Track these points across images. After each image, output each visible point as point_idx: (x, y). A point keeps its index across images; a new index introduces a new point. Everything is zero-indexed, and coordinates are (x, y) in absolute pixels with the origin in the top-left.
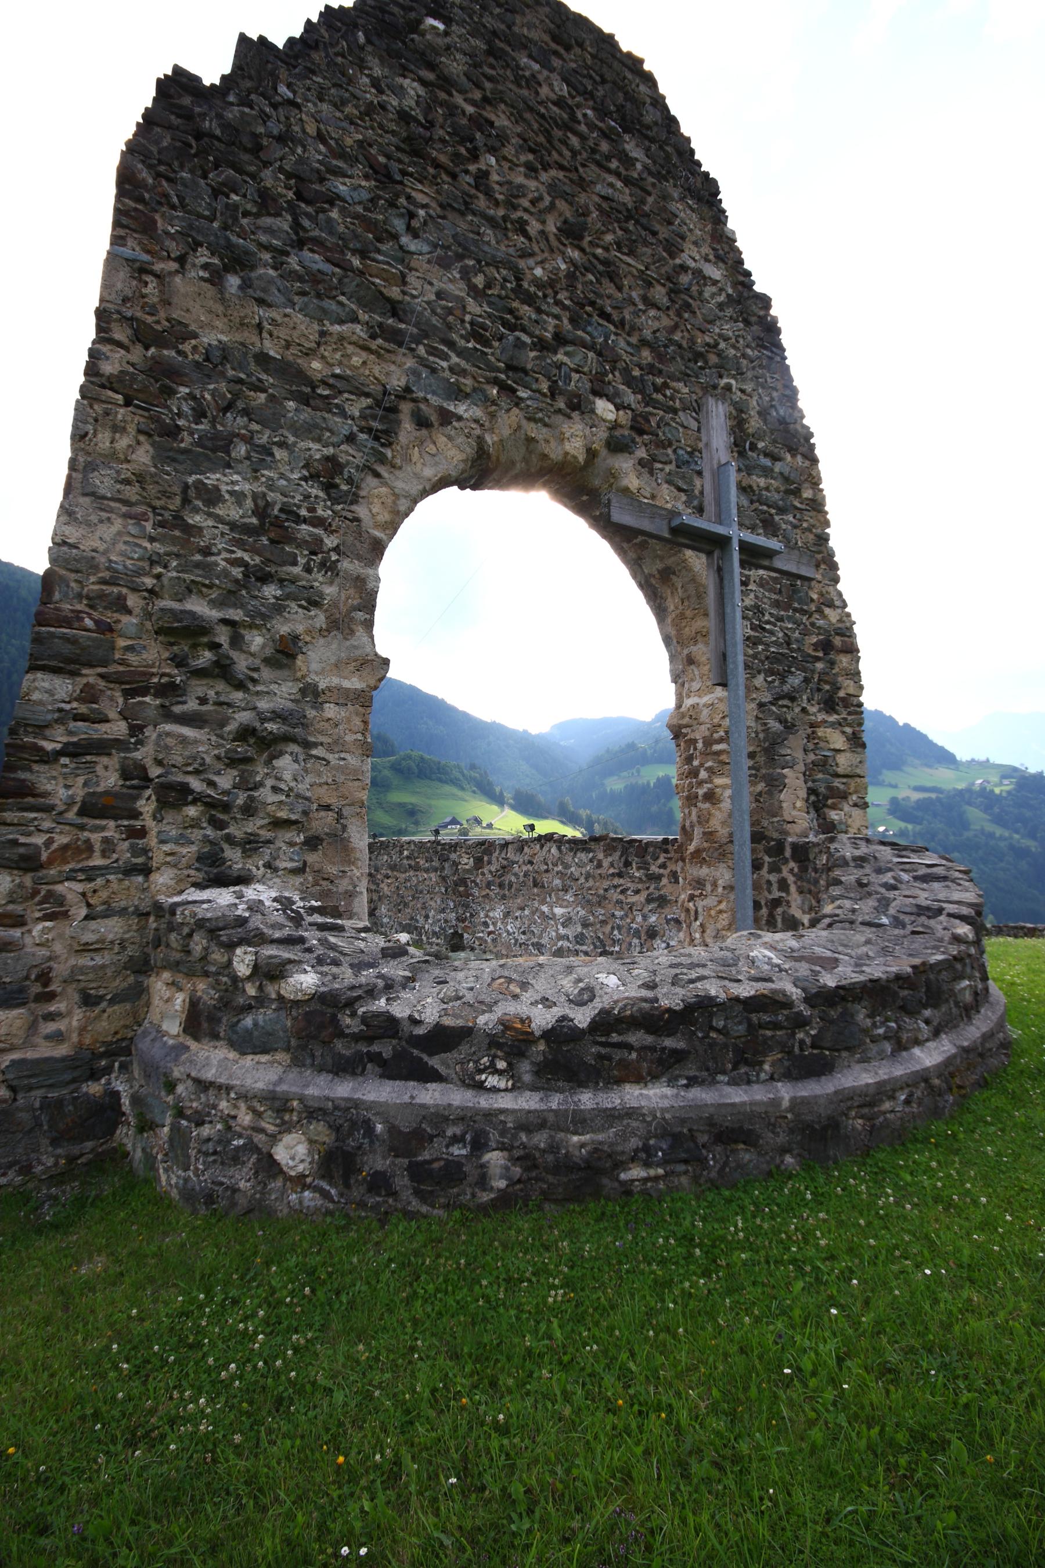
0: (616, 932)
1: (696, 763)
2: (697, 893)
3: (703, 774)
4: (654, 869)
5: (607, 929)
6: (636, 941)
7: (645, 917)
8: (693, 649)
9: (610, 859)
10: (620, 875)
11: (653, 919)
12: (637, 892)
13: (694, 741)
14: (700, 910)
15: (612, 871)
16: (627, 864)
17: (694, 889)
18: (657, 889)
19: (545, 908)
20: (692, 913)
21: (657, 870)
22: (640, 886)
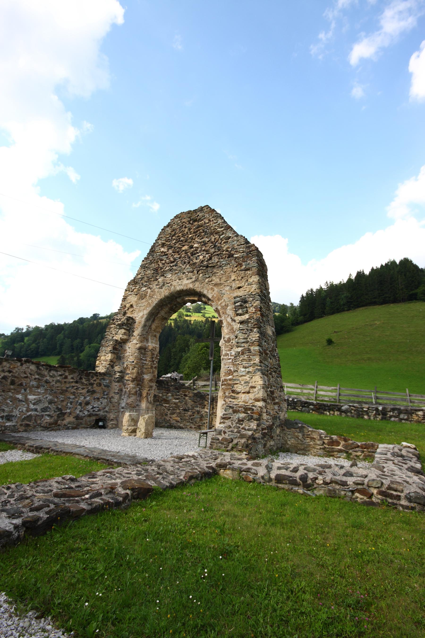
0: (69, 404)
1: (154, 359)
3: (155, 362)
5: (64, 403)
6: (79, 407)
7: (85, 398)
8: (157, 334)
9: (71, 376)
10: (77, 382)
11: (88, 398)
12: (83, 389)
13: (154, 354)
15: (72, 380)
16: (81, 378)
18: (92, 388)
19: (20, 396)
21: (93, 382)
22: (85, 387)
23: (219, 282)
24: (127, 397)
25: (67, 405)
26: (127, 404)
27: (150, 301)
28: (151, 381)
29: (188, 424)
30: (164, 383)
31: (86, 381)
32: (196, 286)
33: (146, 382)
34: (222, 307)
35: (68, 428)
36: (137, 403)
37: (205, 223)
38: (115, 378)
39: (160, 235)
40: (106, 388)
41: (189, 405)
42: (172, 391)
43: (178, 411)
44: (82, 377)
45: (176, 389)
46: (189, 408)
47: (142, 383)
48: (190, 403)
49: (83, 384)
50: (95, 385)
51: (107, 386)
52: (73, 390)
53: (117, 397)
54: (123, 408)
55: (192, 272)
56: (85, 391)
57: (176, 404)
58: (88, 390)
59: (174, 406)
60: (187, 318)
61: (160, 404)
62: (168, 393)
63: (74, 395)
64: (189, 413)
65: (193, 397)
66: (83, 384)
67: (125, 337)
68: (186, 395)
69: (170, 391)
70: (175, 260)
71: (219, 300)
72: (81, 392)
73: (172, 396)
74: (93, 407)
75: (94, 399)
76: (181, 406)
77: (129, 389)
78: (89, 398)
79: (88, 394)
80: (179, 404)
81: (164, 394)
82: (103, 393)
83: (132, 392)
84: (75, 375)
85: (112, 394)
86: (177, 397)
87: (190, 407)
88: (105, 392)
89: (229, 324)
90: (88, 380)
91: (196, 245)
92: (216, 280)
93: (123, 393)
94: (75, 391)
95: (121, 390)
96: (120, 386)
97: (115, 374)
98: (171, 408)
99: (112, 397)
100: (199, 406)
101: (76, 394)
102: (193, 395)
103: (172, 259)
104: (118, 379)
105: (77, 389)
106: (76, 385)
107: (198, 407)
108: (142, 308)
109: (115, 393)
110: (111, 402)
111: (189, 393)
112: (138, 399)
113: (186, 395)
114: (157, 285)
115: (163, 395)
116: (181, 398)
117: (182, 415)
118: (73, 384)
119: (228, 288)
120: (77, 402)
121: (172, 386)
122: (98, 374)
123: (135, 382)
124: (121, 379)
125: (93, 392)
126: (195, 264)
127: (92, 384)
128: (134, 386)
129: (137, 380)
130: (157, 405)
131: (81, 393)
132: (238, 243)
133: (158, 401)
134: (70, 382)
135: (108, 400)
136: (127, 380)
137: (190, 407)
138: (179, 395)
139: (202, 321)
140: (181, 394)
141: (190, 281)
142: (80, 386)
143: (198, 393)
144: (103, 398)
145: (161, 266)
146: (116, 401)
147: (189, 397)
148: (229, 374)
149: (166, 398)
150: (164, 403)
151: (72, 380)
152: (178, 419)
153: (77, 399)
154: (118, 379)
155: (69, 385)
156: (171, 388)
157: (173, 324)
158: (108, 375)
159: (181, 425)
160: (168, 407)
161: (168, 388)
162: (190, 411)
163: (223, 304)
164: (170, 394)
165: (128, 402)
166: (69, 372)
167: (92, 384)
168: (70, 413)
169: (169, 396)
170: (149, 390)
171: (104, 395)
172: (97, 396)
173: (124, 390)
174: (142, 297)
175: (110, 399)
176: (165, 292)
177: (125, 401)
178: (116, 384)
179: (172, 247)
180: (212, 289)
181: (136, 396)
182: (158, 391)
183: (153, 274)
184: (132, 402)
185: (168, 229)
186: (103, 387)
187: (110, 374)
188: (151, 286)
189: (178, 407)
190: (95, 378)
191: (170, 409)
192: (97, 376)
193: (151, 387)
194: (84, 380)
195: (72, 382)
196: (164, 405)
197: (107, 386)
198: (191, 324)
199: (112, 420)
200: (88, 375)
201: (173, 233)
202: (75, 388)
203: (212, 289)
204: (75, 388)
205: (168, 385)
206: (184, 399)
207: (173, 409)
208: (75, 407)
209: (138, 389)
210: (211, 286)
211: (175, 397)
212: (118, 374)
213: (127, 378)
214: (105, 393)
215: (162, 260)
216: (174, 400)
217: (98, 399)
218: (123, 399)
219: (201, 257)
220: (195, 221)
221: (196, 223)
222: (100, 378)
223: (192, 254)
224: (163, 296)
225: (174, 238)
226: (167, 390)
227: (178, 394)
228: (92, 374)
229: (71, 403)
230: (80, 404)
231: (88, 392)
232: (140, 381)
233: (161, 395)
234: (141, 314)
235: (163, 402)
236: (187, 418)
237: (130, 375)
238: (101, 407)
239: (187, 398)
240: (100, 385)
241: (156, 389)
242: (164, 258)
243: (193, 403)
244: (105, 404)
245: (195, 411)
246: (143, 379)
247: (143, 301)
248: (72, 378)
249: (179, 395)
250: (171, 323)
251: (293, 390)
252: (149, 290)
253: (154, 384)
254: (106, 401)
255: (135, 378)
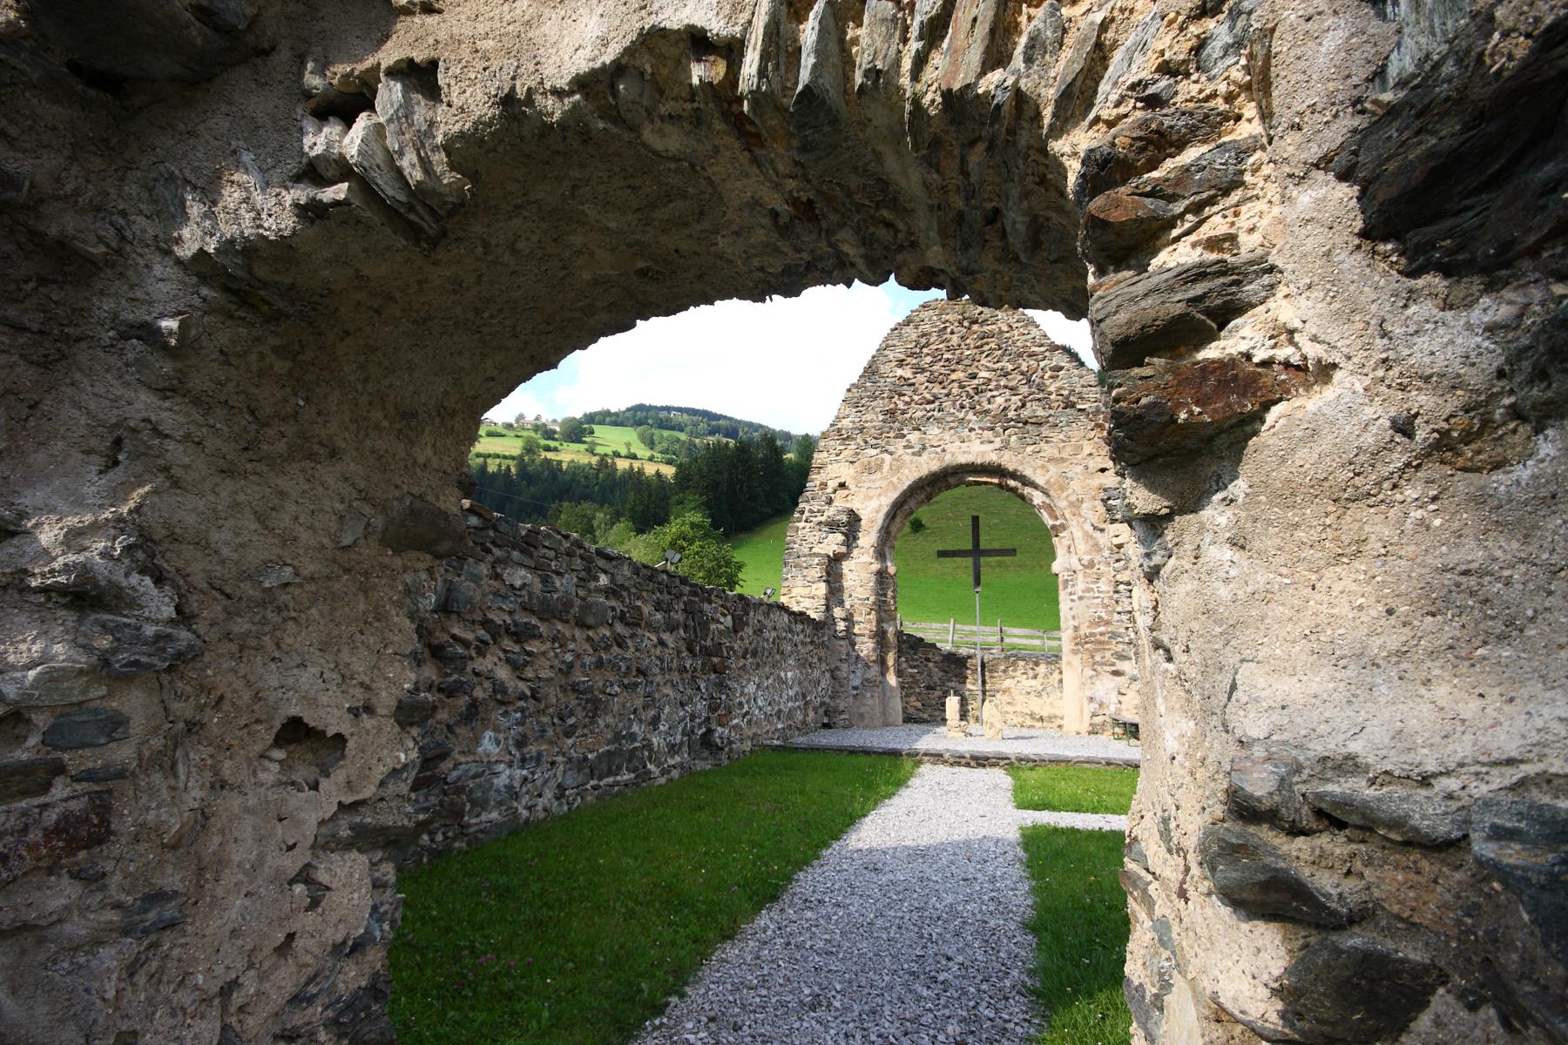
23: (1057, 455)
27: (895, 480)
32: (1006, 457)
34: (1071, 504)
37: (1001, 332)
39: (887, 339)
45: (911, 647)
48: (937, 674)
54: (855, 688)
55: (992, 429)
60: (550, 455)
64: (938, 693)
67: (844, 549)
68: (928, 660)
70: (936, 398)
71: (1062, 489)
89: (1088, 536)
91: (983, 374)
92: (1048, 450)
99: (837, 668)
103: (929, 397)
108: (873, 492)
113: (928, 660)
114: (905, 447)
119: (1079, 469)
126: (987, 412)
132: (1082, 382)
139: (590, 464)
141: (991, 447)
145: (901, 406)
148: (1098, 625)
152: (919, 704)
157: (513, 470)
159: (925, 716)
163: (1073, 498)
174: (870, 469)
176: (928, 464)
177: (859, 674)
179: (924, 370)
180: (1043, 467)
183: (884, 421)
185: (907, 329)
188: (891, 449)
189: (916, 682)
198: (560, 470)
201: (923, 341)
203: (1043, 467)
210: (1040, 462)
215: (901, 395)
219: (1000, 400)
220: (976, 322)
221: (975, 327)
223: (977, 391)
224: (924, 472)
225: (925, 350)
234: (874, 504)
242: (908, 391)
247: (872, 477)
250: (508, 468)
251: (1024, 641)
252: (887, 457)
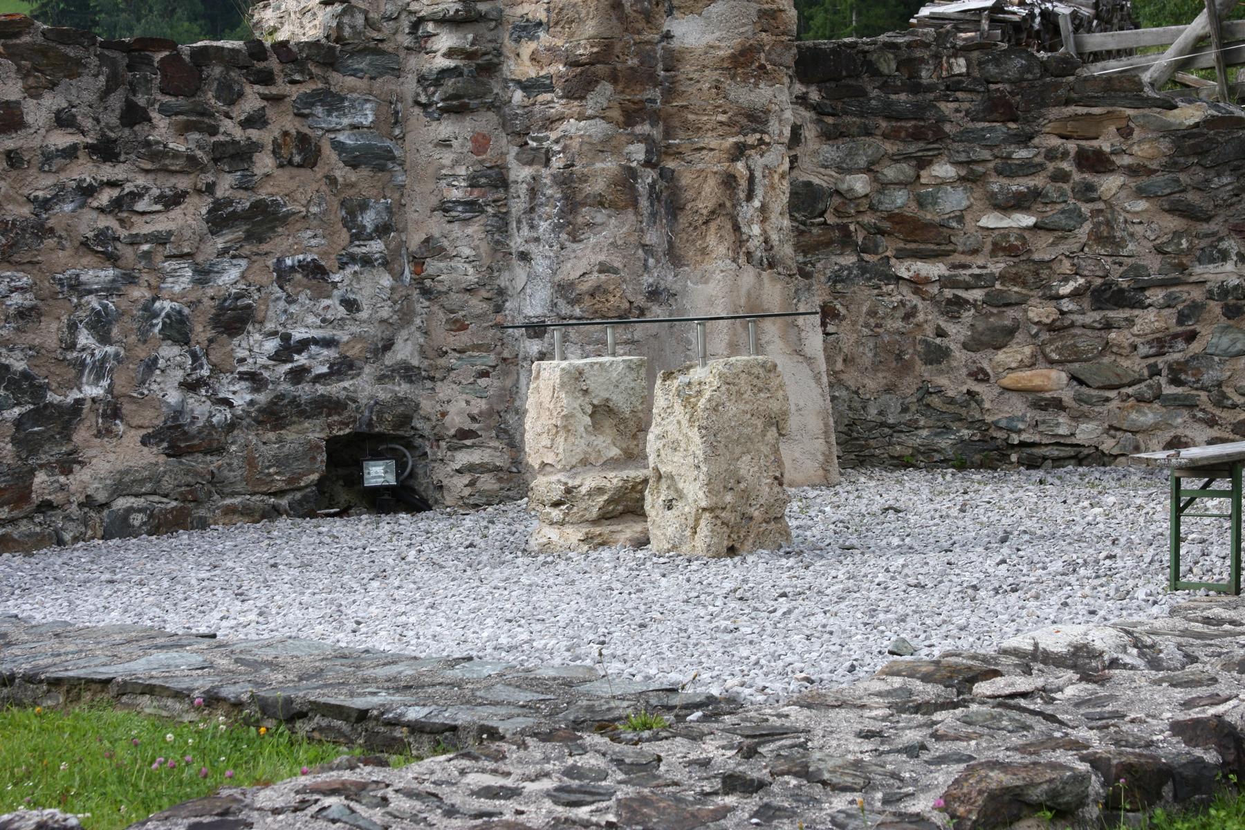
0: (84, 338)
2: (752, 139)
4: (231, 129)
5: (49, 333)
6: (169, 352)
7: (203, 275)
10: (105, 151)
11: (230, 276)
12: (172, 201)
14: (758, 174)
15: (62, 140)
16: (134, 115)
17: (743, 131)
20: (743, 184)
21: (238, 134)
22: (183, 183)
24: (557, 228)
25: (72, 346)
26: (563, 289)
28: (743, 62)
29: (1148, 416)
30: (875, 73)
31: (183, 130)
33: (699, 85)
35: (120, 528)
36: (647, 279)
38: (421, 79)
40: (365, 172)
41: (1139, 250)
42: (966, 136)
43: (1039, 311)
44: (141, 100)
45: (999, 109)
46: (1137, 270)
47: (670, 92)
48: (1145, 226)
49: (157, 157)
50: (264, 162)
51: (374, 159)
52: (90, 222)
53: (467, 240)
56: (187, 219)
57: (1011, 251)
58: (217, 205)
59: (997, 267)
61: (863, 268)
62: (923, 163)
63: (112, 259)
64: (1150, 320)
65: (1172, 165)
66: (157, 157)
68: (1096, 162)
69: (941, 136)
72: (161, 224)
73: (970, 179)
74: (288, 349)
75: (283, 275)
76: (1066, 266)
77: (557, 162)
78: (233, 274)
79: (220, 243)
80: (1043, 248)
81: (890, 172)
82: (350, 221)
83: (598, 186)
84: (83, 91)
85: (422, 225)
86: (1019, 185)
87: (1153, 264)
88: (364, 206)
90: (201, 121)
93: (518, 206)
94: (105, 222)
95: (500, 181)
96: (480, 143)
97: (421, 44)
98: (977, 295)
99: (432, 248)
100: (1232, 245)
101: (127, 252)
102: (1165, 146)
104: (450, 84)
105: (117, 205)
106: (108, 172)
107: (1224, 256)
109: (444, 207)
110: (426, 292)
111: (1125, 133)
112: (651, 238)
113: (1096, 162)
115: (883, 186)
116: (1051, 189)
117: (1086, 341)
118: (85, 171)
120: (149, 312)
121: (953, 86)
122: (274, 63)
123: (606, 88)
124: (471, 85)
125: (263, 220)
127: (239, 156)
128: (597, 128)
129: (614, 78)
130: (836, 279)
131: (161, 239)
133: (846, 240)
134: (48, 158)
135: (398, 277)
136: (530, 87)
137: (1153, 264)
138: (1028, 168)
140: (1051, 155)
142: (141, 180)
143: (1209, 122)
144: (353, 259)
146: (472, 276)
147: (1132, 171)
149: (912, 210)
150: (901, 255)
151: (62, 140)
152: (1054, 379)
153: (139, 293)
154: (450, 84)
155: (50, 180)
156: (947, 107)
158: (363, 64)
159: (1087, 433)
160: (944, 282)
161: (918, 112)
162: (1156, 295)
164: (943, 170)
165: (571, 271)
166: (25, 74)
167: (239, 156)
168: (113, 412)
169: (941, 183)
170: (739, 151)
171: (359, 235)
172: (298, 245)
173: (521, 173)
175: (418, 262)
177: (541, 265)
178: (445, 128)
181: (630, 216)
182: (829, 151)
184: (604, 268)
186: (342, 173)
187: (374, 50)
189: (1036, 277)
190: (251, 101)
191: (959, 303)
192: (266, 78)
193: (755, 119)
194: (161, 129)
195: (70, 153)
196: (903, 269)
197: (374, 159)
199: (463, 434)
200: (185, 77)
202: (105, 197)
204: (105, 197)
205: (915, 87)
206: (1087, 194)
207: (990, 300)
208: (142, 352)
209: (638, 152)
211: (996, 184)
212: (445, 40)
213: (527, 70)
214: (369, 219)
216: (991, 220)
217: (315, 271)
218: (524, 257)
222: (294, 92)
226: (917, 136)
227: (1022, 154)
228: (217, 71)
229: (101, 325)
230: (178, 330)
231: (219, 219)
232: (643, 76)
233: (859, 184)
235: (889, 246)
236: (1135, 365)
237: (544, 38)
238: (356, 338)
239: (1110, 184)
240: (303, 152)
241: (810, 132)
243: (1173, 223)
244: (385, 313)
245: (1197, 294)
246: (673, 60)
248: (63, 120)
249: (1028, 168)
253: (779, 97)
254: (386, 281)
255: (594, 60)
